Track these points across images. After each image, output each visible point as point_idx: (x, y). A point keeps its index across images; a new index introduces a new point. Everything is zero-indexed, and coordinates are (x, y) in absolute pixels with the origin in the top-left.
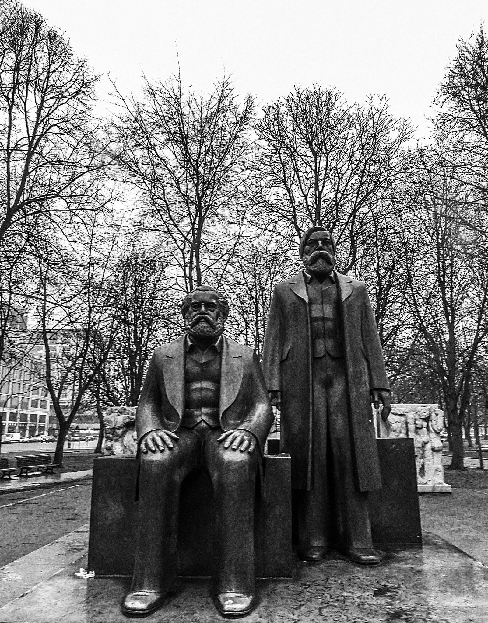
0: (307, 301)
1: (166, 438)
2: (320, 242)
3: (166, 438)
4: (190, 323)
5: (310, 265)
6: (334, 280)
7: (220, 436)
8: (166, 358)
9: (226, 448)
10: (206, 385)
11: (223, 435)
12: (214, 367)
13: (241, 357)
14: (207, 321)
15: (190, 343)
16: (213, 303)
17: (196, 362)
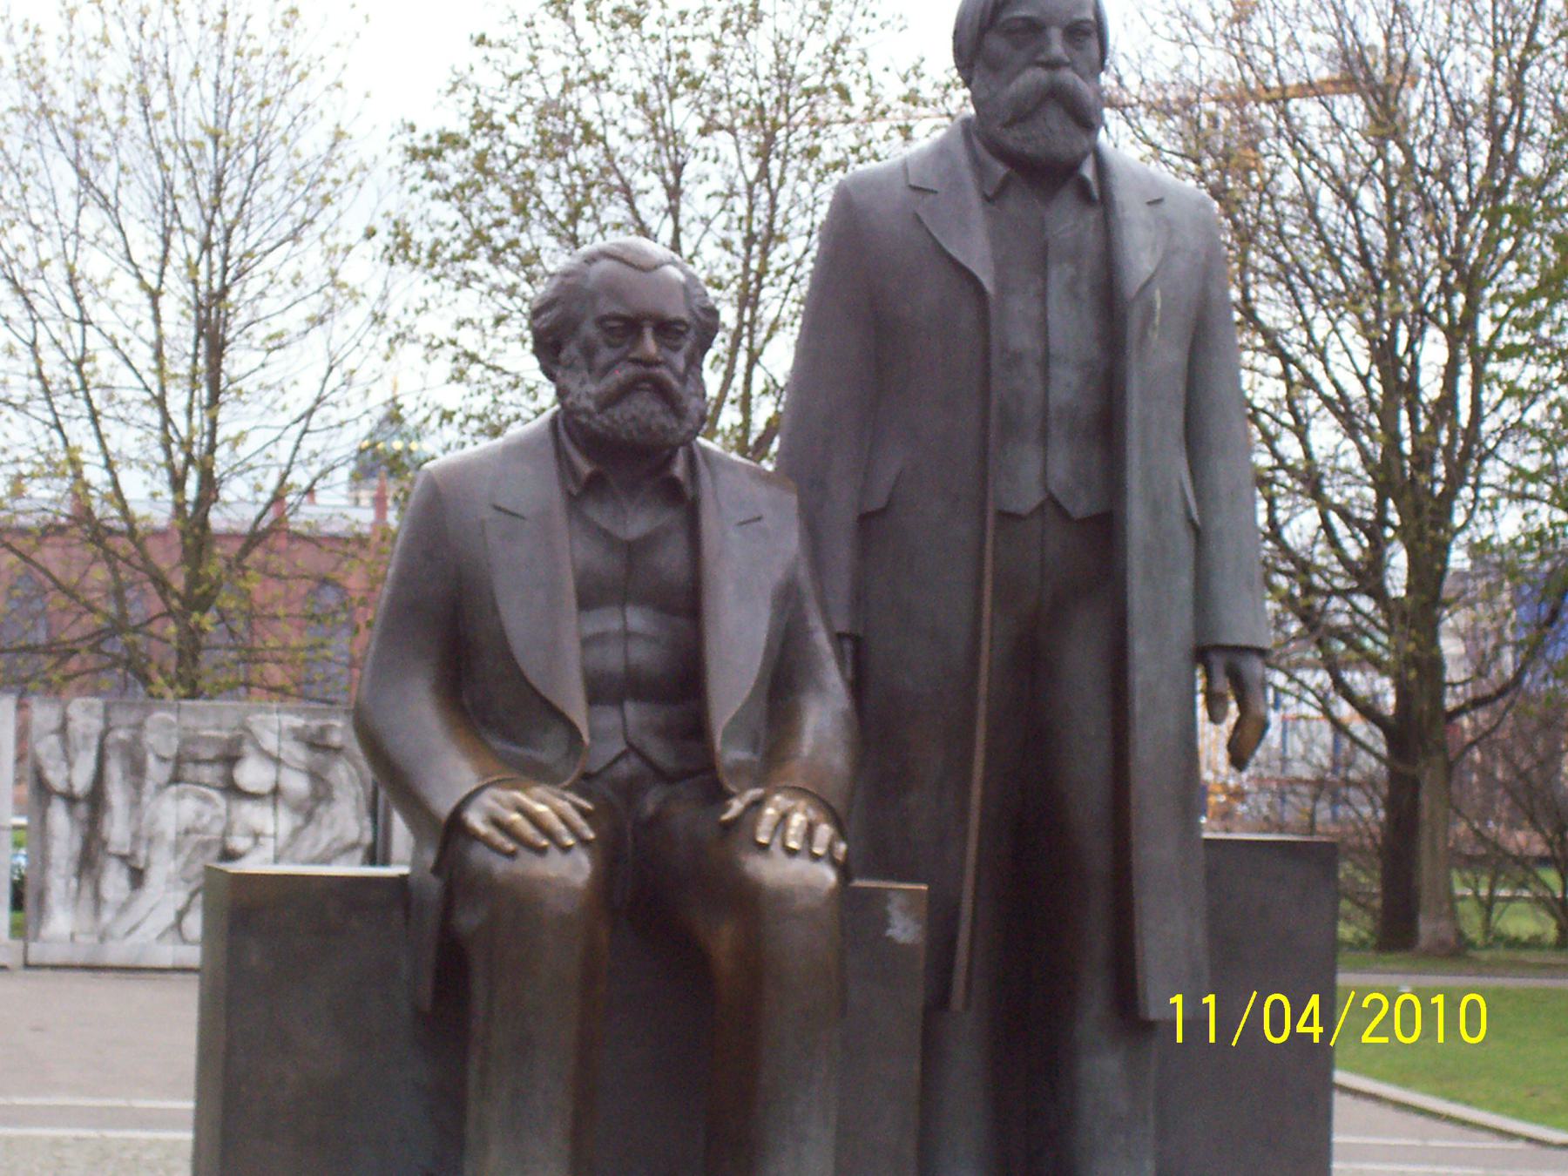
0: (989, 287)
1: (564, 806)
2: (1055, 34)
3: (564, 806)
4: (592, 388)
5: (1008, 125)
6: (1096, 193)
7: (726, 809)
8: (488, 514)
9: (764, 848)
10: (637, 619)
11: (736, 806)
12: (671, 558)
13: (759, 519)
14: (662, 391)
15: (585, 468)
16: (681, 322)
17: (606, 535)
